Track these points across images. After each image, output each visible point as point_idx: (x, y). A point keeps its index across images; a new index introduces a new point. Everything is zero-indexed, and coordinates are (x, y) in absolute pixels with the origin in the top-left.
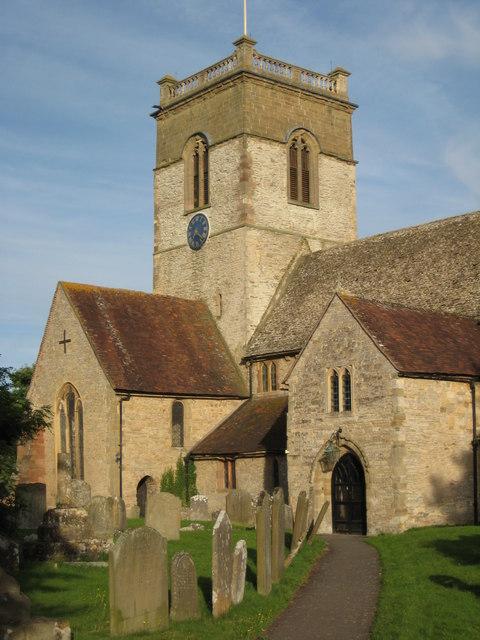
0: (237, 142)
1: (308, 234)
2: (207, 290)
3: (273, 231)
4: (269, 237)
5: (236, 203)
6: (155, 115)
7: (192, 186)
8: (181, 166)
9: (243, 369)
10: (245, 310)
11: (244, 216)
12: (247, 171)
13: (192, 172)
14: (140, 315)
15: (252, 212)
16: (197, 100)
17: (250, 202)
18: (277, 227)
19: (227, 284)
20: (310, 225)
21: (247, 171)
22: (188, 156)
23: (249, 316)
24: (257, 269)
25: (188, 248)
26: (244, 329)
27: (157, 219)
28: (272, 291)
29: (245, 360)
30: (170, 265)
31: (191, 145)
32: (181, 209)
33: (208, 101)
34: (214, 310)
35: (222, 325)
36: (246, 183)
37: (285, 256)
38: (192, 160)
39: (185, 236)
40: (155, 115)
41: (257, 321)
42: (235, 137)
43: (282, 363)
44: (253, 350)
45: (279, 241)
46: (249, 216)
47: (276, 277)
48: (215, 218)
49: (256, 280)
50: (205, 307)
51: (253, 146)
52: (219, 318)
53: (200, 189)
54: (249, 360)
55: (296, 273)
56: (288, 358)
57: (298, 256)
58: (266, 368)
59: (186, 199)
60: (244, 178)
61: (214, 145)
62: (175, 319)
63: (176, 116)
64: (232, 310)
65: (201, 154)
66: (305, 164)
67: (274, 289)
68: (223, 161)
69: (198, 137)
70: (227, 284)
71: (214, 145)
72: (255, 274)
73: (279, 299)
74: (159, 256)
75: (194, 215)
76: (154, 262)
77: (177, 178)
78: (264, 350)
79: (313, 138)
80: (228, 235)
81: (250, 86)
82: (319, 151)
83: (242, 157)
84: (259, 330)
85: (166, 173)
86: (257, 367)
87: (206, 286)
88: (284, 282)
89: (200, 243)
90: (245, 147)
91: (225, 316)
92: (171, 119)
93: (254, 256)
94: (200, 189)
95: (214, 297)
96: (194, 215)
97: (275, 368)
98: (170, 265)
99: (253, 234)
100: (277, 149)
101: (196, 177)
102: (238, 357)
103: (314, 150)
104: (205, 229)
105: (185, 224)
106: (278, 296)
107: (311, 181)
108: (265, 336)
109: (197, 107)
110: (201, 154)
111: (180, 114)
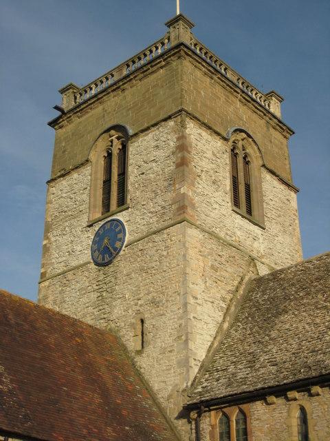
0: (171, 123)
1: (254, 254)
2: (119, 318)
3: (218, 238)
4: (212, 245)
5: (170, 196)
6: (54, 123)
7: (100, 192)
8: (87, 170)
9: (182, 425)
10: (184, 336)
11: (182, 209)
12: (186, 154)
13: (101, 177)
14: (26, 327)
15: (193, 206)
16: (115, 93)
17: (190, 194)
18: (222, 235)
19: (155, 303)
20: (256, 245)
21: (186, 154)
22: (97, 157)
23: (191, 345)
24: (200, 281)
25: (93, 266)
26: (185, 364)
27: (48, 238)
28: (219, 316)
29: (186, 412)
30: (62, 292)
31: (102, 145)
32: (84, 220)
33: (127, 92)
34: (132, 343)
35: (143, 362)
36: (186, 168)
37: (233, 275)
38: (102, 162)
39: (89, 252)
40: (54, 123)
41: (201, 354)
42: (169, 118)
43: (258, 408)
44: (200, 394)
45: (226, 253)
46: (189, 210)
47: (224, 299)
48: (132, 221)
49: (199, 296)
50: (117, 339)
51: (193, 130)
52: (139, 353)
53: (115, 191)
54: (194, 409)
55: (247, 298)
56: (272, 399)
57: (247, 278)
58: (227, 418)
59: (91, 207)
60: (182, 163)
61: (136, 135)
62: (79, 344)
63: (81, 119)
64: (163, 336)
65: (115, 151)
66: (247, 174)
67: (221, 314)
68: (149, 155)
69: (113, 132)
70: (155, 303)
71: (136, 135)
72: (197, 287)
73: (228, 330)
74: (47, 283)
75: (102, 223)
76: (40, 291)
77: (81, 187)
78: (221, 391)
79: (256, 148)
80: (157, 238)
81: (186, 65)
82: (261, 163)
83: (178, 139)
84: (205, 368)
85: (64, 183)
86: (210, 421)
87: (118, 311)
88: (233, 309)
89: (111, 255)
90: (183, 126)
91: (149, 350)
92: (69, 128)
93: (197, 264)
94: (115, 191)
95: (132, 326)
96: (102, 223)
97: (244, 417)
98: (62, 292)
99: (193, 234)
100: (219, 143)
101: (107, 183)
102: (173, 408)
103: (256, 163)
104: (120, 236)
105: (88, 238)
106: (226, 325)
107: (254, 195)
108: (216, 375)
109: (112, 101)
110: (115, 151)
111: (87, 116)
